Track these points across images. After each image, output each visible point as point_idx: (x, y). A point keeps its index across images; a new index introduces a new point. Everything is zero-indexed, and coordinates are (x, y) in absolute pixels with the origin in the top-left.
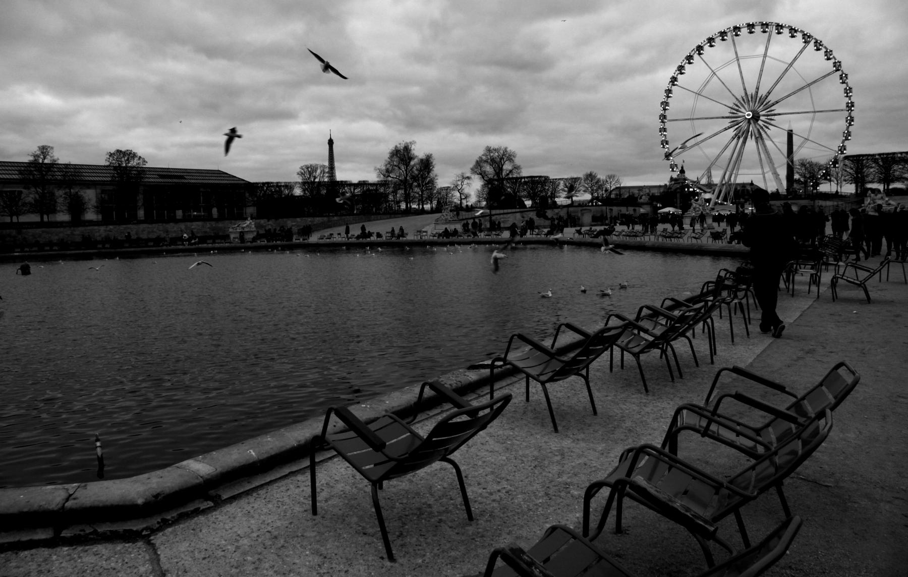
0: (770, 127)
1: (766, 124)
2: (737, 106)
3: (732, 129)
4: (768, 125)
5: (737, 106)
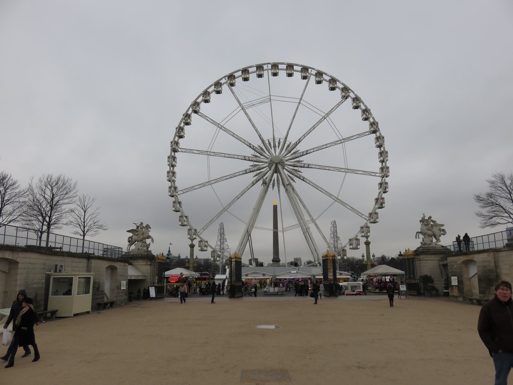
0: (276, 187)
1: (276, 181)
2: (279, 143)
3: (253, 152)
4: (276, 184)
5: (279, 143)
